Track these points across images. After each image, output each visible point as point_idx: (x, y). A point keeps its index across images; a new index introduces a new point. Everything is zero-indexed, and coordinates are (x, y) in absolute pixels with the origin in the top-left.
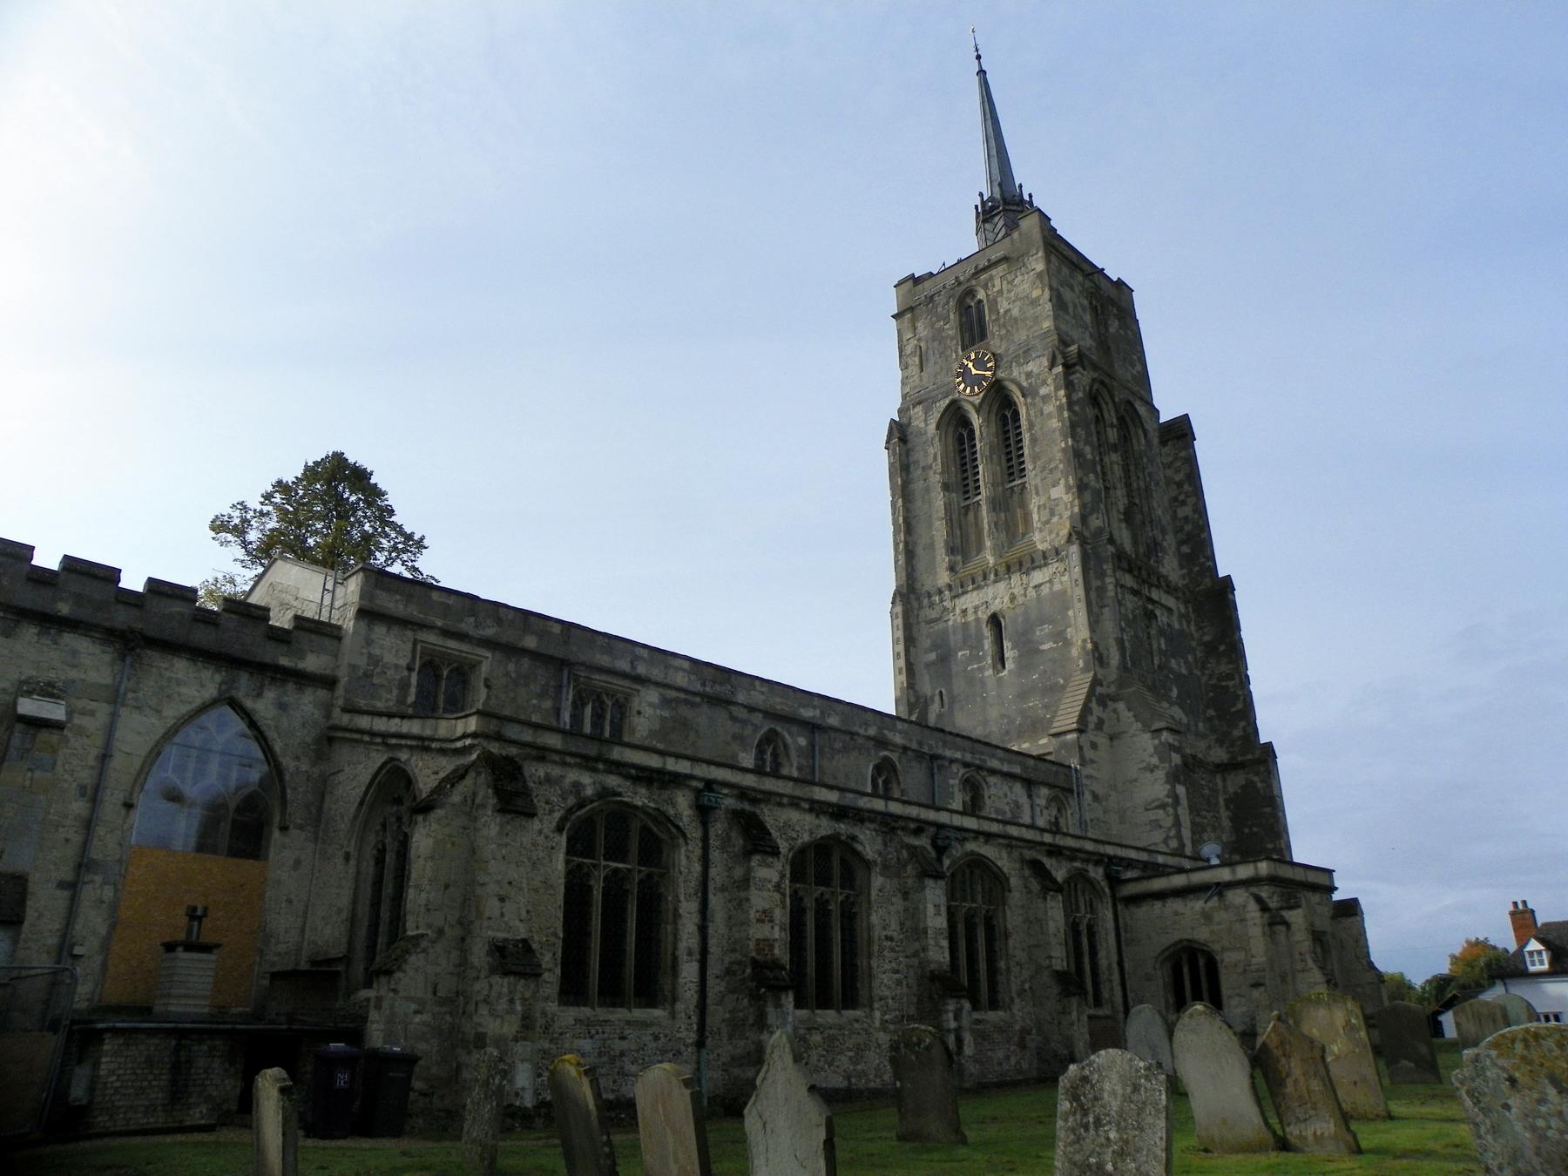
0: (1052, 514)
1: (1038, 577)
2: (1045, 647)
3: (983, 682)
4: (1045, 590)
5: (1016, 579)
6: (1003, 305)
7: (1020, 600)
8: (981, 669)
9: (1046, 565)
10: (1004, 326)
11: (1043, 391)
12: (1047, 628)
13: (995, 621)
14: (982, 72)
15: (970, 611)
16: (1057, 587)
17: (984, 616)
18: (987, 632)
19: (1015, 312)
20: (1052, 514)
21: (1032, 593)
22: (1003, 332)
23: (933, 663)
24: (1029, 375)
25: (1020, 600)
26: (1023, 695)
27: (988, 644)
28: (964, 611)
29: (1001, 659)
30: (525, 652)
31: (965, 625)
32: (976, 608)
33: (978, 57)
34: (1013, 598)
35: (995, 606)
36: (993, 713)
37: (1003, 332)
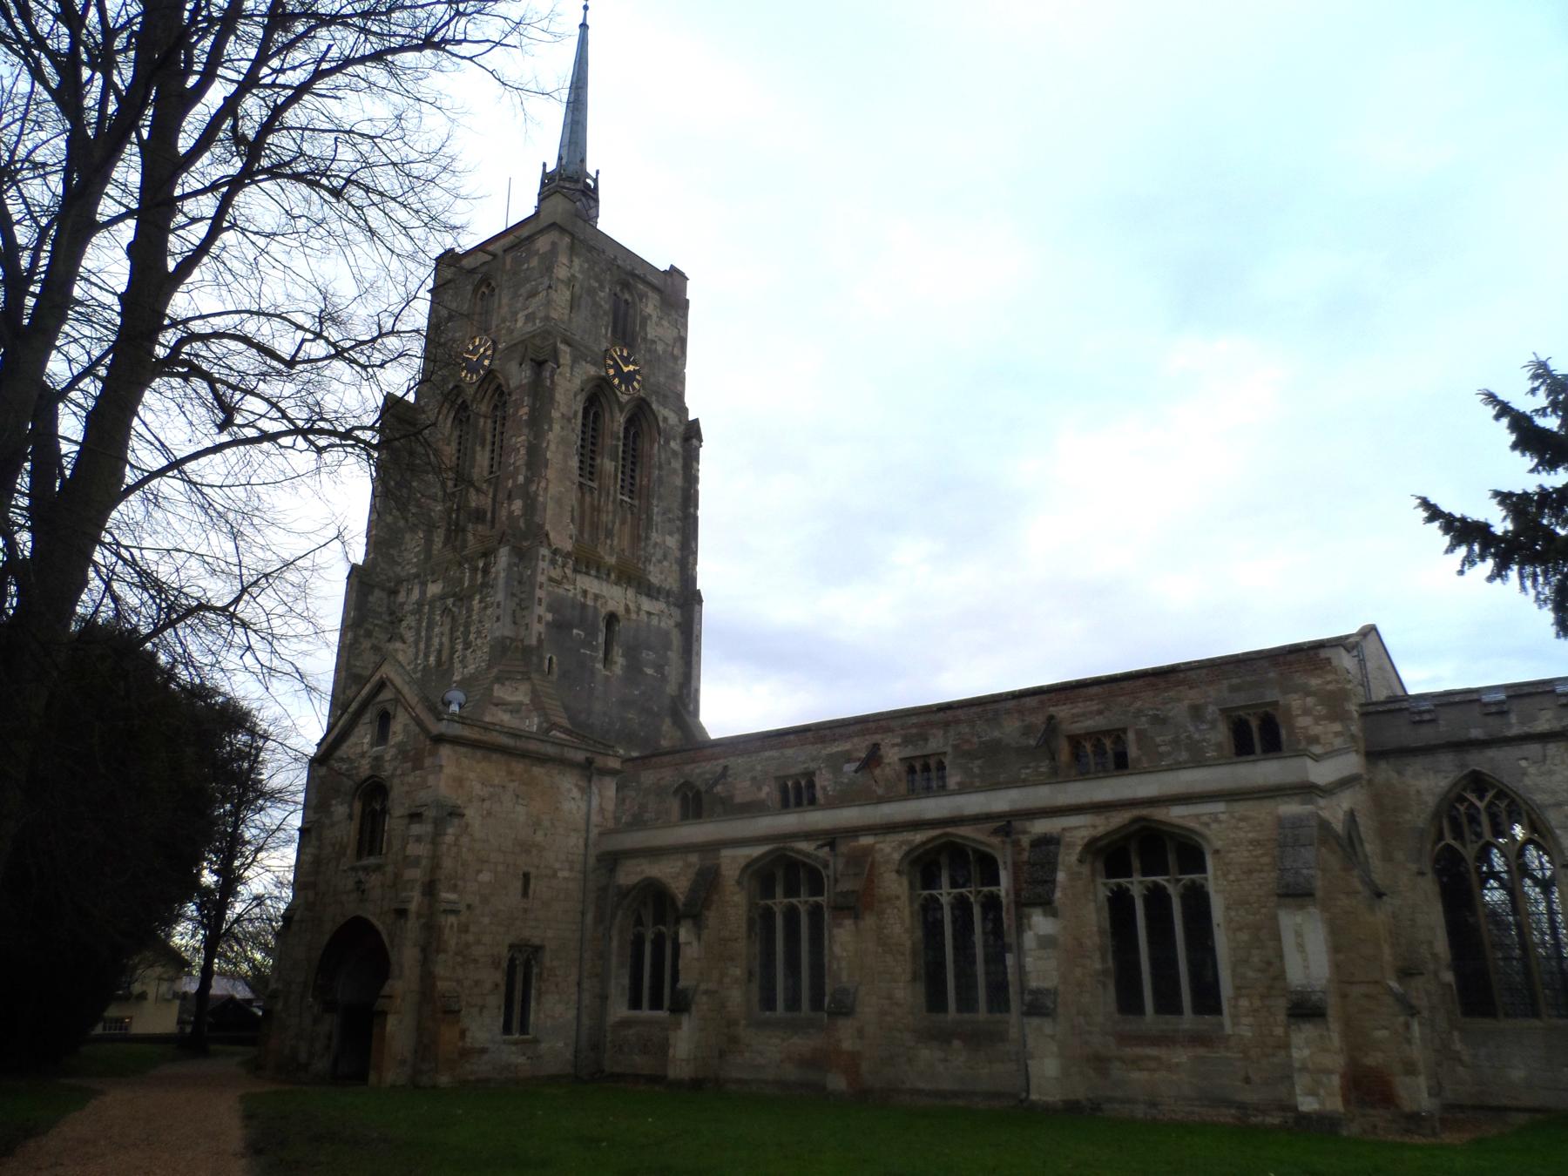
1: (647, 604)
3: (593, 672)
4: (655, 621)
8: (593, 659)
11: (672, 444)
12: (652, 656)
13: (612, 618)
14: (584, 26)
15: (590, 596)
17: (603, 612)
18: (602, 626)
19: (660, 348)
20: (665, 557)
21: (644, 616)
24: (665, 419)
25: (634, 616)
27: (601, 638)
28: (585, 593)
29: (607, 660)
31: (584, 606)
32: (596, 597)
33: (586, 8)
34: (627, 610)
35: (611, 606)
36: (598, 707)
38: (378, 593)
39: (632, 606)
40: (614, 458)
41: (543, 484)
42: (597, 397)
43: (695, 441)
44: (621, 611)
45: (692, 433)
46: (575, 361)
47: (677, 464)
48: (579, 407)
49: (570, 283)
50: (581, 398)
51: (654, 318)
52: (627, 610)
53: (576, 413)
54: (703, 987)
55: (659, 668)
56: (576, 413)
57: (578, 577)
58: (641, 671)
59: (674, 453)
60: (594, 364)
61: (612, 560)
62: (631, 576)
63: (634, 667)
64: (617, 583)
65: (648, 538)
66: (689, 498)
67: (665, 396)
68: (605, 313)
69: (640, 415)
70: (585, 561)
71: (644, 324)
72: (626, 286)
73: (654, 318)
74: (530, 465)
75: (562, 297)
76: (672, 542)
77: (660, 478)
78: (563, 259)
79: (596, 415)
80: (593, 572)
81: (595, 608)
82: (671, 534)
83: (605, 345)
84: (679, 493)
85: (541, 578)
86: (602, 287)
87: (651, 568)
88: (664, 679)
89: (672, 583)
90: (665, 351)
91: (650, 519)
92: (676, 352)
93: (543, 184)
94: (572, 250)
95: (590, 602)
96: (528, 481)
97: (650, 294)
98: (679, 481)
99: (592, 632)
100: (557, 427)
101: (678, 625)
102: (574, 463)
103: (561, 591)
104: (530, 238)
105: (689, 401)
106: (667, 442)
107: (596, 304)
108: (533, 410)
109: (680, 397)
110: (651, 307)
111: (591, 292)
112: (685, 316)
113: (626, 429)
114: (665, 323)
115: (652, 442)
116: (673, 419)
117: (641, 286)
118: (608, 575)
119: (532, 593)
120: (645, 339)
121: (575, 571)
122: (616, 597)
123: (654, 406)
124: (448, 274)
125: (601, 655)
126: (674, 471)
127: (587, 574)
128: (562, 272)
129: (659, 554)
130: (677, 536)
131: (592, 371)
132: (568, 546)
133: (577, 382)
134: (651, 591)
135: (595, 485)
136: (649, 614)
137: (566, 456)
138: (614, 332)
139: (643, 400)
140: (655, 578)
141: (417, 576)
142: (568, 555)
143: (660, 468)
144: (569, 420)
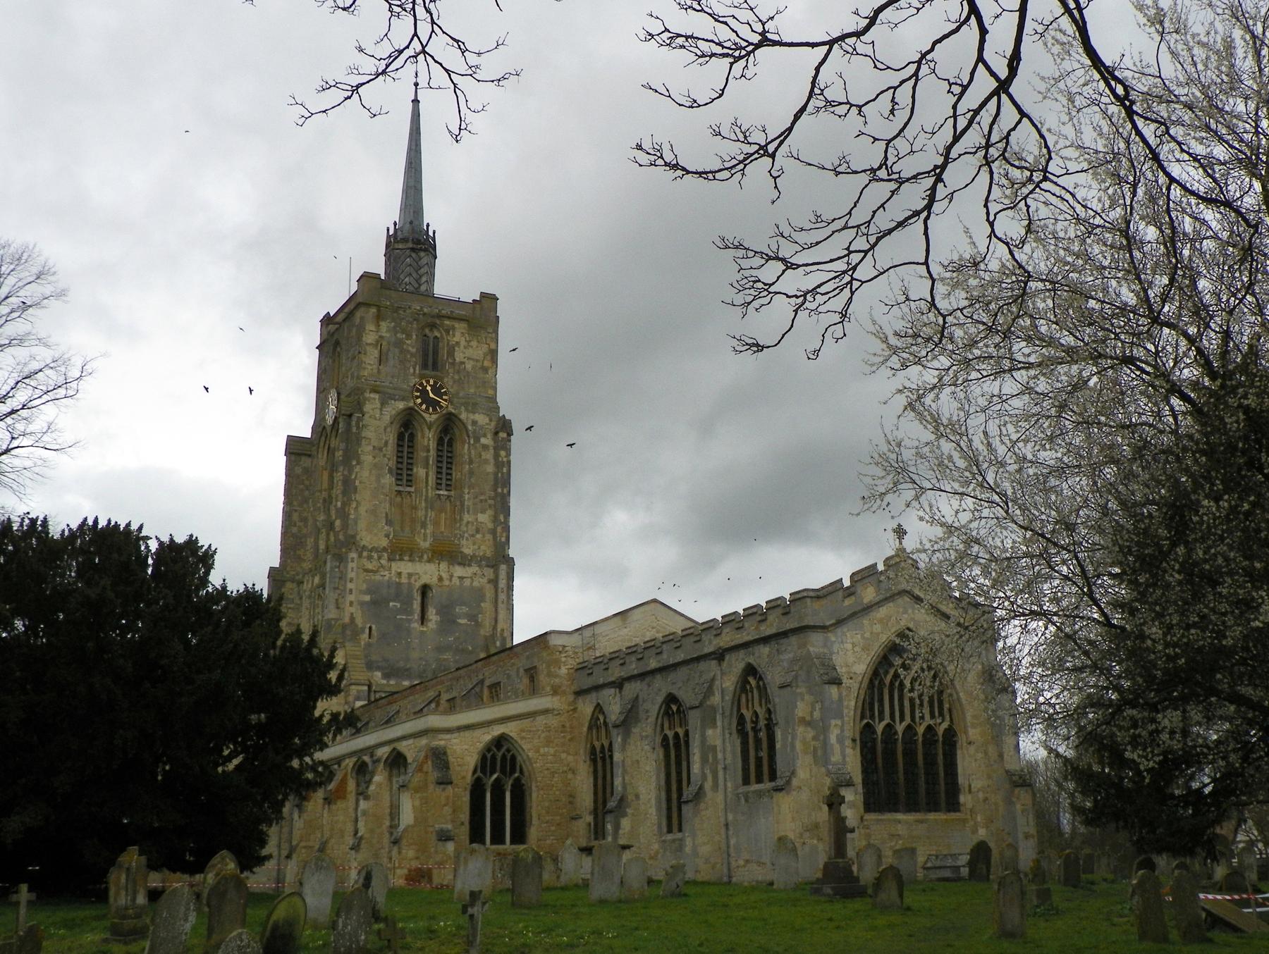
0: (478, 531)
1: (459, 571)
2: (460, 621)
4: (467, 583)
5: (444, 565)
6: (459, 356)
7: (446, 583)
8: (409, 621)
9: (470, 565)
10: (458, 372)
11: (483, 440)
12: (465, 609)
13: (425, 589)
16: (476, 584)
17: (418, 585)
19: (469, 366)
21: (456, 581)
22: (457, 377)
23: (367, 603)
24: (474, 423)
25: (446, 583)
26: (439, 649)
27: (416, 605)
28: (400, 574)
29: (423, 619)
30: (653, 672)
32: (410, 575)
34: (441, 579)
35: (425, 579)
36: (415, 655)
37: (457, 377)
38: (289, 585)
39: (444, 575)
40: (426, 466)
41: (354, 505)
42: (407, 426)
43: (503, 435)
44: (433, 581)
45: (505, 426)
46: (383, 404)
47: (489, 455)
48: (392, 438)
49: (378, 343)
50: (395, 427)
51: (463, 343)
52: (441, 579)
53: (386, 443)
54: (303, 844)
55: (473, 617)
56: (386, 443)
57: (393, 564)
58: (454, 622)
59: (485, 447)
60: (403, 399)
61: (425, 545)
62: (446, 553)
63: (448, 620)
64: (429, 561)
65: (461, 519)
66: (502, 482)
67: (475, 405)
68: (412, 355)
69: (449, 428)
70: (399, 550)
71: (451, 353)
72: (433, 326)
73: (463, 343)
74: (345, 493)
75: (371, 356)
76: (485, 518)
77: (471, 473)
78: (370, 327)
79: (412, 436)
80: (406, 558)
81: (410, 584)
82: (483, 512)
83: (414, 380)
84: (492, 477)
85: (351, 575)
86: (409, 336)
87: (464, 542)
88: (478, 625)
89: (486, 549)
90: (473, 367)
91: (462, 505)
92: (486, 364)
93: (387, 246)
94: (379, 318)
95: (404, 580)
96: (344, 504)
97: (457, 325)
98: (490, 468)
99: (408, 602)
100: (367, 459)
101: (490, 581)
102: (388, 480)
103: (378, 577)
104: (351, 313)
105: (501, 399)
106: (477, 440)
107: (402, 351)
108: (346, 451)
109: (493, 399)
110: (459, 334)
111: (398, 344)
112: (496, 332)
113: (440, 442)
114: (474, 343)
115: (463, 442)
116: (481, 419)
117: (447, 322)
118: (421, 557)
119: (345, 586)
120: (453, 364)
121: (390, 560)
122: (428, 572)
123: (463, 416)
124: (332, 328)
125: (416, 616)
126: (486, 462)
127: (401, 559)
128: (370, 338)
129: (472, 529)
130: (490, 512)
131: (401, 405)
132: (384, 543)
133: (387, 418)
134: (465, 561)
135: (412, 489)
136: (461, 578)
137: (378, 477)
138: (425, 366)
139: (451, 414)
140: (468, 550)
141: (311, 570)
142: (385, 549)
143: (471, 462)
144: (381, 449)
